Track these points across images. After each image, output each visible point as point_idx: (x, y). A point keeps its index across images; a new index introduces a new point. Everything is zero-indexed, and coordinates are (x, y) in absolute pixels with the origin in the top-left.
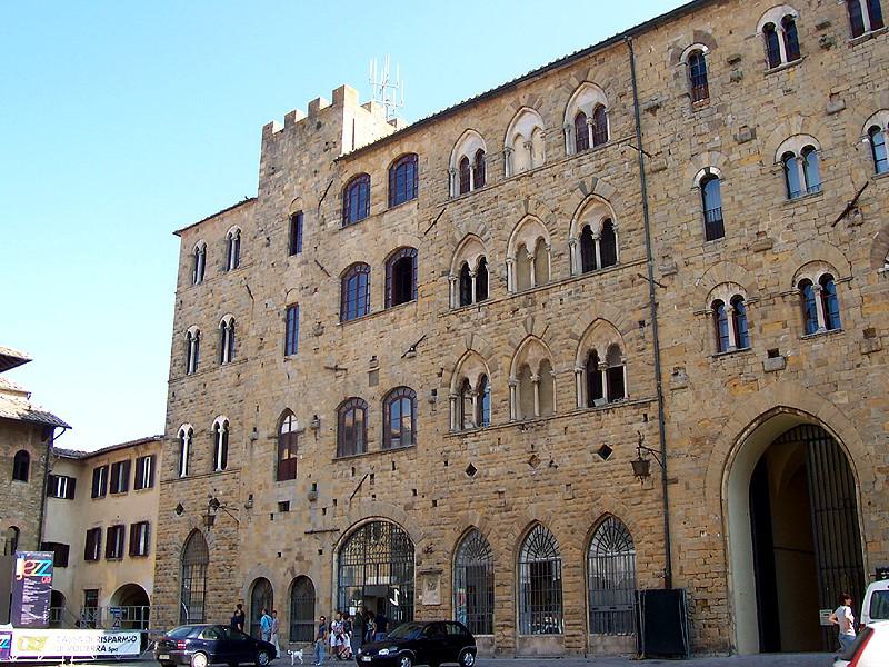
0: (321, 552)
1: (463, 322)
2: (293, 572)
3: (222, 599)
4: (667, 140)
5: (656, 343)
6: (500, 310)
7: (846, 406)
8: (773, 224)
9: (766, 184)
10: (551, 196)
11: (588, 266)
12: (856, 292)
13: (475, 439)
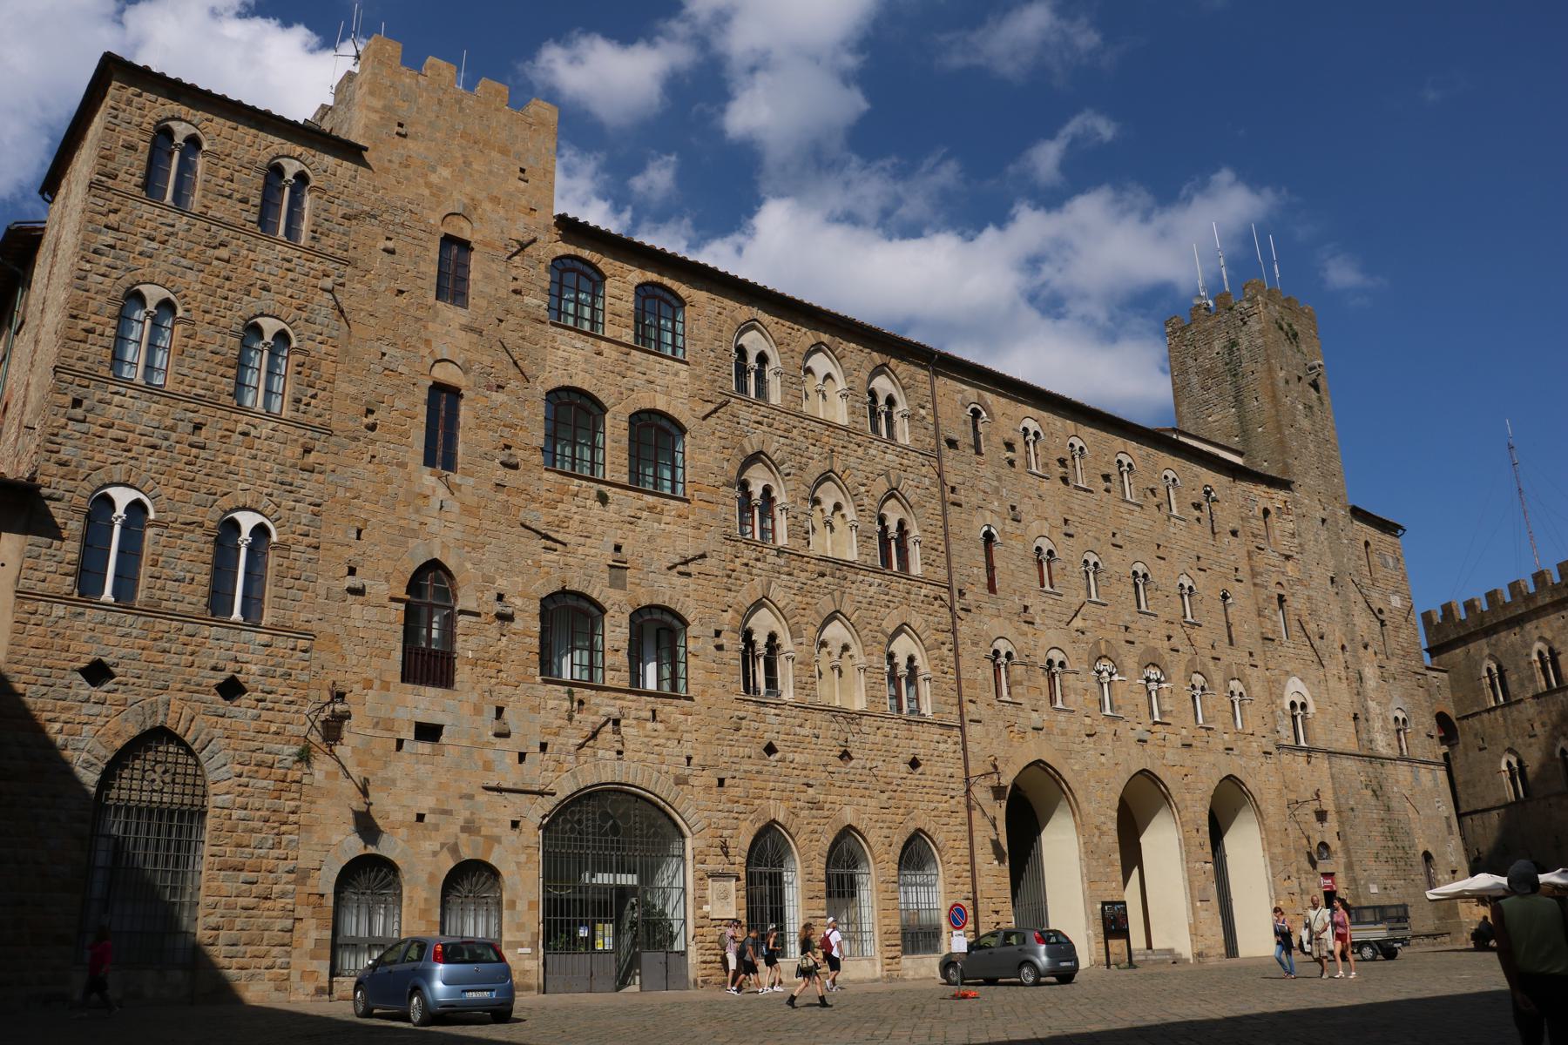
0: (515, 824)
1: (758, 560)
2: (454, 850)
4: (960, 479)
13: (777, 711)
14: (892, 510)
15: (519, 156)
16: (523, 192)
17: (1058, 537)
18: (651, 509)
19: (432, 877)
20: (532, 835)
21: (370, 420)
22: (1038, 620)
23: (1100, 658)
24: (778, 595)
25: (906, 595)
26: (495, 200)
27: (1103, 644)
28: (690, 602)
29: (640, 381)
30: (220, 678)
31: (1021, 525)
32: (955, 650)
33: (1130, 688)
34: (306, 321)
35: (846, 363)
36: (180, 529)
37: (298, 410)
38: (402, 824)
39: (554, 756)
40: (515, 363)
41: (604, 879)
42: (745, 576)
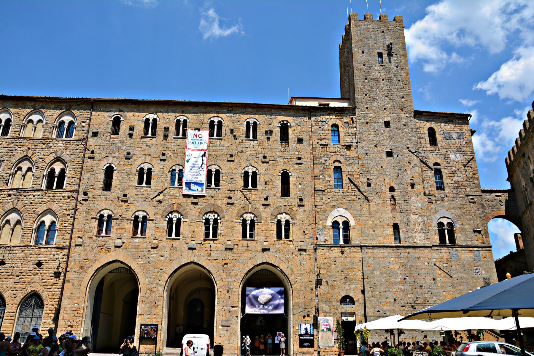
4: (97, 147)
7: (142, 264)
8: (130, 193)
9: (132, 177)
10: (39, 152)
11: (50, 185)
12: (154, 225)
14: (58, 165)
22: (132, 199)
23: (171, 212)
25: (53, 198)
27: (175, 206)
33: (190, 224)
35: (45, 114)
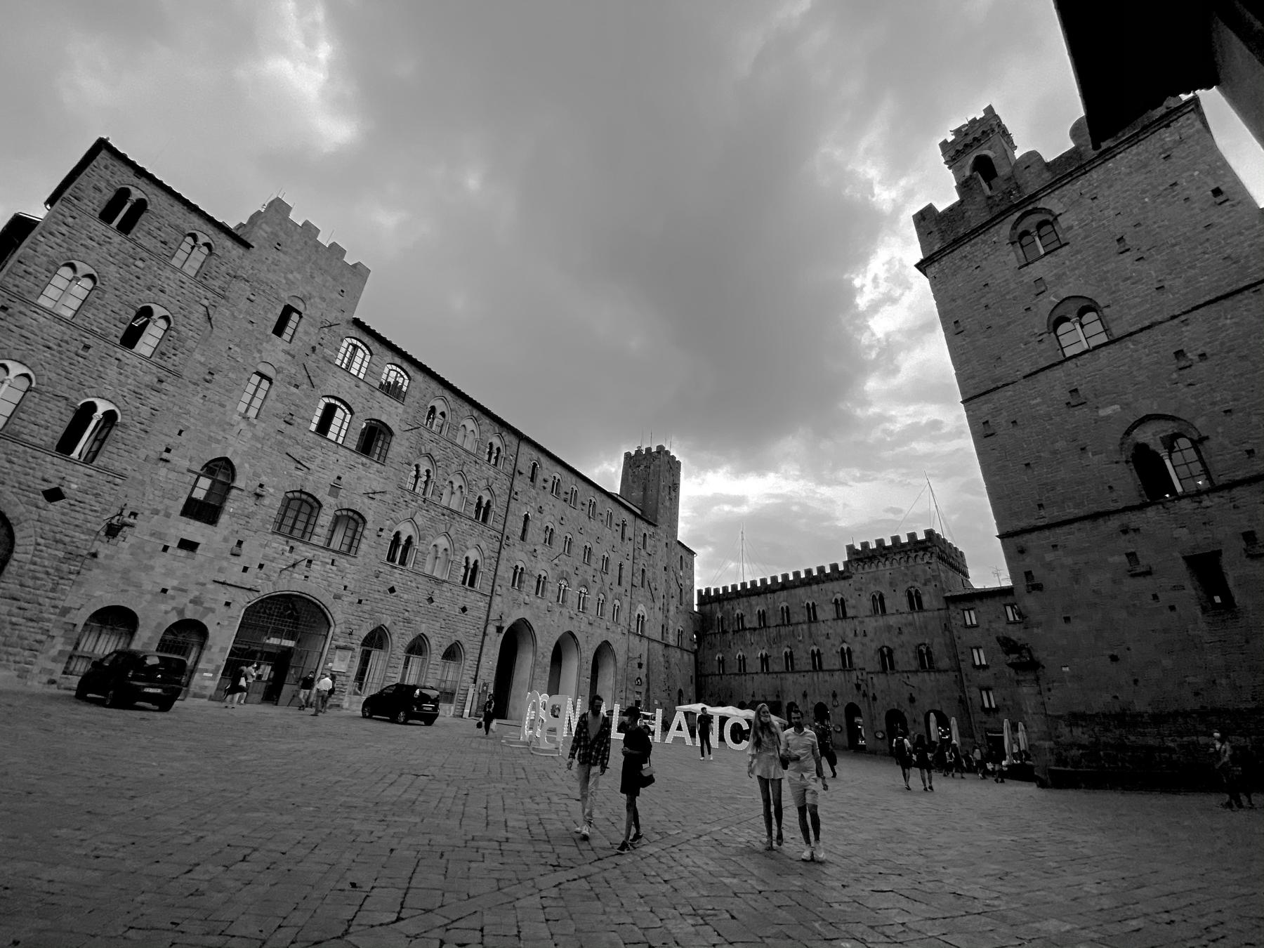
1: (413, 501)
3: (28, 614)
5: (496, 570)
6: (436, 509)
14: (486, 495)
15: (342, 284)
16: (339, 300)
17: (557, 524)
18: (363, 464)
19: (159, 625)
20: (238, 612)
21: (208, 377)
22: (539, 557)
24: (419, 520)
26: (323, 299)
28: (371, 512)
29: (376, 405)
30: (46, 487)
31: (542, 515)
32: (498, 562)
34: (184, 316)
36: (51, 398)
37: (161, 359)
38: (150, 592)
39: (268, 573)
40: (309, 377)
41: (274, 641)
42: (405, 507)
